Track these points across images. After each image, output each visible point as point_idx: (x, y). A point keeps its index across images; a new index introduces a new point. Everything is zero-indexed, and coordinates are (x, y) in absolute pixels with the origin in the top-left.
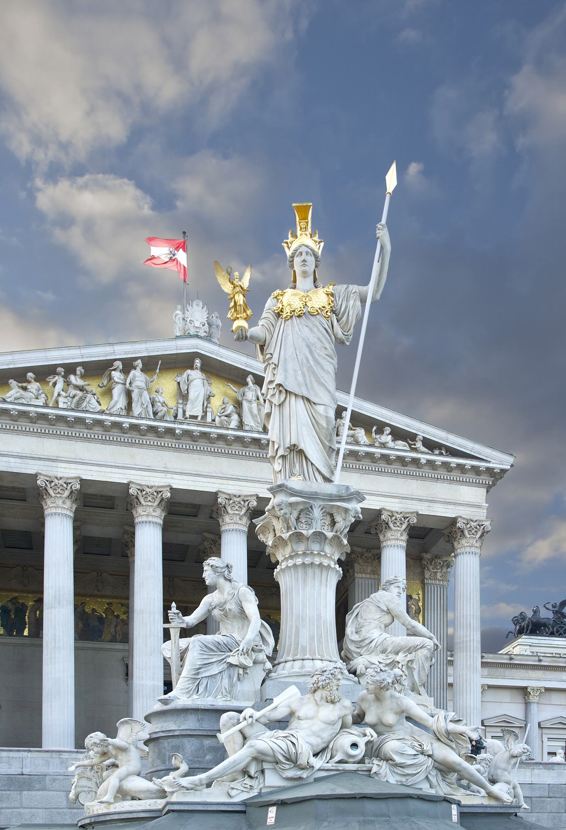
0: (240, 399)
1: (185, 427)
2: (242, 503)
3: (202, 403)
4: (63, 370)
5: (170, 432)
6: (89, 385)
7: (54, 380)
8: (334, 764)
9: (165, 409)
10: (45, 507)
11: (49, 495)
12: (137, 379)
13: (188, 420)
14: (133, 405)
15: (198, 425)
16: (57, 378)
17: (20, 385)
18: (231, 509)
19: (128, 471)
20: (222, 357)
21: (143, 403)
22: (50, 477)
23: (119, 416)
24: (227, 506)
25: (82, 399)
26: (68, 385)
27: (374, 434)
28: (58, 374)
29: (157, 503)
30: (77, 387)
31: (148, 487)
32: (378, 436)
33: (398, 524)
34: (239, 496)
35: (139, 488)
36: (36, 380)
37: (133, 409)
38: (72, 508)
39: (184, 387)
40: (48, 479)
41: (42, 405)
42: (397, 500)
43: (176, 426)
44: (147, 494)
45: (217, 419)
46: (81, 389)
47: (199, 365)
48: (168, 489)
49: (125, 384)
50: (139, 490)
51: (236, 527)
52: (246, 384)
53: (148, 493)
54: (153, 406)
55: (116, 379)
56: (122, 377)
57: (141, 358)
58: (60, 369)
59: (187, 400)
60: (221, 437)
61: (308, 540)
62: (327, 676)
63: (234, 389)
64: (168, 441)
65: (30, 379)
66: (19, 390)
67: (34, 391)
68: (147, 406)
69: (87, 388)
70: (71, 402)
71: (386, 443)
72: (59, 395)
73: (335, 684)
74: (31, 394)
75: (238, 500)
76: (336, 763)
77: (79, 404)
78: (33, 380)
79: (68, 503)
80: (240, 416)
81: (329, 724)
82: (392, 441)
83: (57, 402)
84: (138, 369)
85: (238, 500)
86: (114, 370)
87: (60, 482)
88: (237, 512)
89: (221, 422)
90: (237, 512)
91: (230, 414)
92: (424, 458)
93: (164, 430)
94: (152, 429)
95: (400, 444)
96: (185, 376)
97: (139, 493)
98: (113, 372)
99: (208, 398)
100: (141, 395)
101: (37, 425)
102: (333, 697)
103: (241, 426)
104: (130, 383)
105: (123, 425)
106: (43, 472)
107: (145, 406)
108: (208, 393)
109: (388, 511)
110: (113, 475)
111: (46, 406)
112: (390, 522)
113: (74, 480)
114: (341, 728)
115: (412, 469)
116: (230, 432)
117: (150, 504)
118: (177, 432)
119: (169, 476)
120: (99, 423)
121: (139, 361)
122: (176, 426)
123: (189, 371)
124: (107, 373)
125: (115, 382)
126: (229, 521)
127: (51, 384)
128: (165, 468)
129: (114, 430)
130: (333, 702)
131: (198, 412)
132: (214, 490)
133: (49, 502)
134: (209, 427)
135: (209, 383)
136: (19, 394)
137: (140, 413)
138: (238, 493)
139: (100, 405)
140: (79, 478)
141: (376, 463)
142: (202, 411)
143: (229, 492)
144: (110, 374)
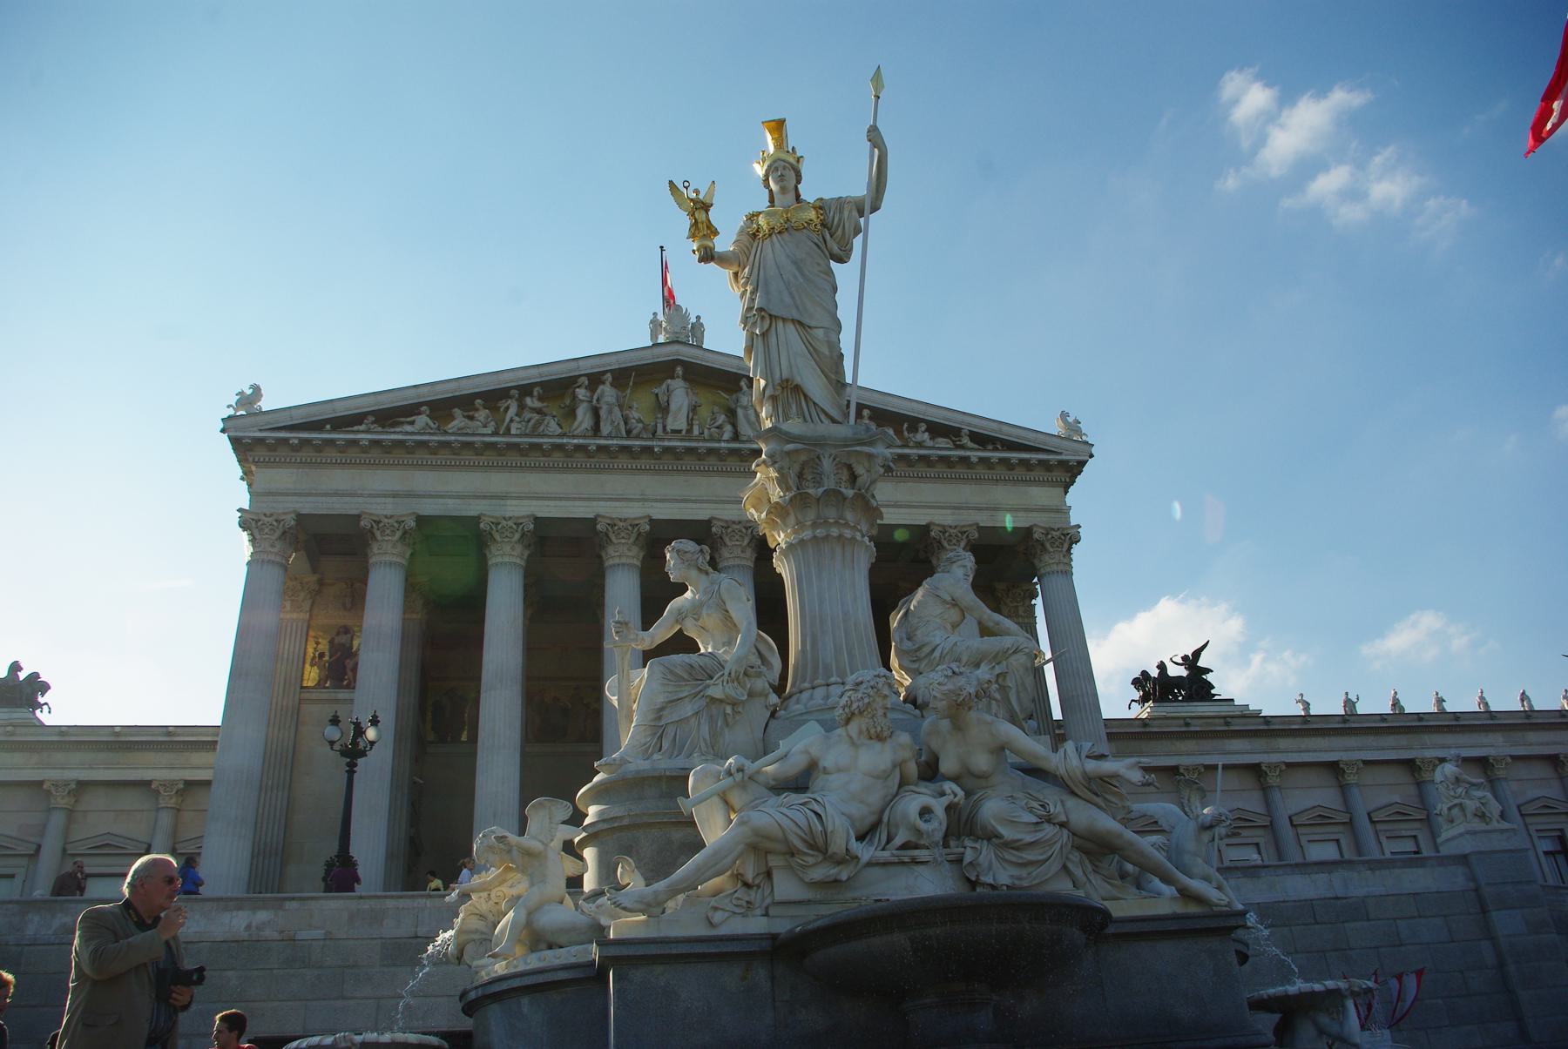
0: (734, 406)
1: (666, 443)
2: (744, 530)
3: (686, 415)
4: (516, 392)
5: (648, 450)
6: (547, 406)
7: (506, 405)
8: (895, 852)
9: (640, 425)
10: (489, 556)
11: (495, 540)
12: (606, 394)
14: (602, 424)
15: (681, 440)
16: (509, 401)
17: (466, 414)
18: (730, 540)
19: (595, 503)
20: (707, 362)
22: (496, 518)
23: (584, 437)
24: (724, 536)
25: (539, 423)
26: (523, 409)
27: (906, 433)
28: (511, 397)
29: (632, 540)
30: (534, 410)
31: (621, 520)
32: (911, 435)
33: (954, 541)
34: (740, 522)
35: (609, 522)
36: (485, 408)
38: (523, 555)
39: (662, 399)
40: (493, 520)
41: (490, 432)
42: (949, 511)
43: (655, 443)
45: (706, 431)
46: (539, 411)
47: (680, 373)
48: (647, 520)
49: (591, 402)
50: (609, 525)
51: (738, 562)
52: (741, 389)
54: (626, 423)
55: (580, 397)
56: (588, 394)
57: (610, 371)
58: (513, 392)
59: (668, 413)
60: (711, 451)
61: (818, 504)
62: (865, 691)
63: (725, 396)
64: (644, 462)
65: (478, 406)
66: (464, 419)
67: (482, 420)
68: (618, 424)
69: (544, 410)
70: (526, 427)
71: (924, 441)
72: (512, 420)
73: (880, 705)
74: (478, 423)
75: (738, 527)
76: (897, 849)
77: (535, 427)
78: (481, 408)
79: (519, 548)
80: (734, 426)
81: (878, 777)
82: (931, 439)
83: (508, 429)
84: (608, 383)
85: (738, 527)
86: (579, 387)
87: (509, 522)
88: (737, 543)
89: (711, 435)
90: (737, 543)
91: (721, 425)
92: (975, 455)
94: (625, 449)
95: (942, 442)
96: (664, 386)
97: (610, 529)
98: (577, 390)
99: (694, 409)
100: (610, 412)
101: (483, 457)
102: (879, 729)
103: (736, 437)
104: (598, 400)
105: (590, 448)
106: (488, 513)
107: (616, 423)
108: (694, 403)
109: (938, 525)
111: (495, 434)
112: (943, 540)
113: (527, 519)
114: (900, 786)
115: (960, 470)
116: (723, 445)
117: (623, 541)
118: (656, 450)
120: (559, 447)
121: (609, 375)
122: (655, 443)
123: (669, 381)
124: (571, 390)
126: (728, 555)
127: (502, 409)
129: (577, 455)
130: (880, 738)
131: (681, 424)
132: (706, 517)
133: (493, 548)
134: (698, 441)
135: (694, 393)
136: (463, 424)
137: (611, 432)
138: (735, 518)
139: (561, 428)
140: (533, 515)
141: (913, 466)
142: (686, 423)
143: (726, 518)
144: (574, 391)
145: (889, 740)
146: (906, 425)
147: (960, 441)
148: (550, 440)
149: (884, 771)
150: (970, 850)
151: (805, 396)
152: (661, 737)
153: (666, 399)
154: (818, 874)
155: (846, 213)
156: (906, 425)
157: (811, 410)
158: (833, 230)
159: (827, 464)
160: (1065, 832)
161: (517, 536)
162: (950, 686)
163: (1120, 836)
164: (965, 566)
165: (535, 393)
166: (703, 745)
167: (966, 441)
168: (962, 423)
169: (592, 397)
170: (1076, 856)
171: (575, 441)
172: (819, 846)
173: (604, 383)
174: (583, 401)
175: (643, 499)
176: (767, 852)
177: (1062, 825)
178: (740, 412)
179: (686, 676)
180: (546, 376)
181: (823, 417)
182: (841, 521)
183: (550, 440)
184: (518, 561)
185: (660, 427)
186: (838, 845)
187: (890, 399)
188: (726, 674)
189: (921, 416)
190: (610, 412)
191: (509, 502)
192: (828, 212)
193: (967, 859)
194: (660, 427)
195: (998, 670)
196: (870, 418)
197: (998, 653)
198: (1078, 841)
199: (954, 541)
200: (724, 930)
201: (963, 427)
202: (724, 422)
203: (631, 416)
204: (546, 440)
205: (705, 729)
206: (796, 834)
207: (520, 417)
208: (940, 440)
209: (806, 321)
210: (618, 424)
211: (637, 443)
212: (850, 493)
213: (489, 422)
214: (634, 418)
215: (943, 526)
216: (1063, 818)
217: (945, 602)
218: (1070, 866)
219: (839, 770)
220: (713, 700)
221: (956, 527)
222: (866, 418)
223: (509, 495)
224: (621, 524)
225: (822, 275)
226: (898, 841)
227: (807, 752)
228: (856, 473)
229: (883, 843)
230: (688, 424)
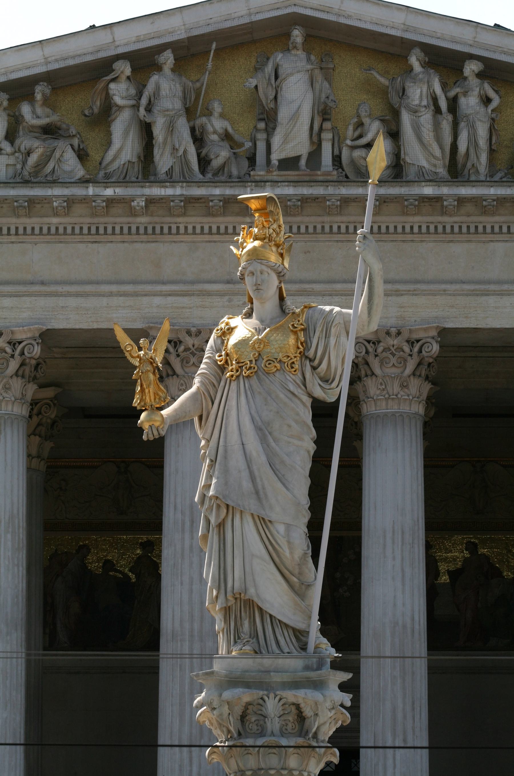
13: (275, 173)
14: (156, 151)
15: (296, 183)
21: (177, 146)
44: (187, 349)
49: (136, 107)
53: (191, 346)
55: (118, 100)
68: (185, 152)
86: (114, 80)
98: (112, 86)
100: (171, 128)
107: (181, 152)
124: (101, 85)
153: (272, 97)
155: (332, 341)
157: (265, 624)
158: (316, 362)
161: (13, 365)
165: (39, 96)
169: (140, 95)
171: (109, 192)
173: (159, 68)
178: (406, 118)
180: (57, 60)
183: (66, 192)
185: (261, 146)
190: (171, 128)
192: (312, 335)
194: (261, 146)
203: (210, 129)
204: (57, 191)
207: (12, 143)
210: (185, 152)
211: (217, 191)
214: (215, 132)
228: (304, 715)
230: (312, 142)
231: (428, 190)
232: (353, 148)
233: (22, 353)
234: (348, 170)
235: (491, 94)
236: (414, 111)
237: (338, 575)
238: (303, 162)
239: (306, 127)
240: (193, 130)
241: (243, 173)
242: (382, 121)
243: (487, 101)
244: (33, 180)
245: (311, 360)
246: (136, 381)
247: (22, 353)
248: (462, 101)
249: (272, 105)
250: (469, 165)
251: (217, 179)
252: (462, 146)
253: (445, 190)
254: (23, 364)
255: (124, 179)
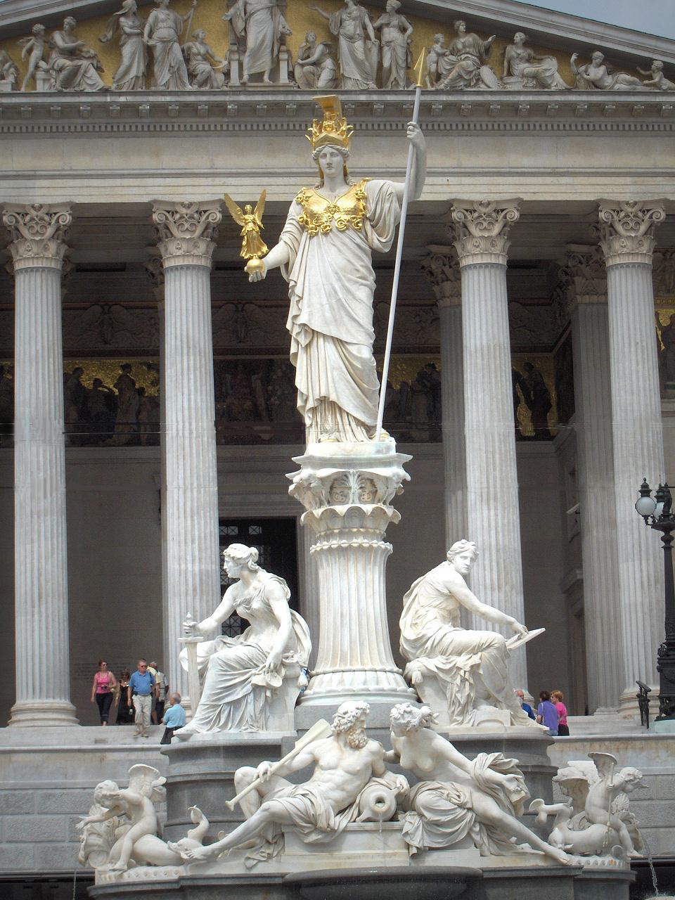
1: (243, 98)
12: (161, 25)
14: (156, 69)
37: (156, 76)
49: (141, 34)
50: (168, 212)
55: (127, 30)
56: (137, 23)
68: (178, 69)
93: (207, 107)
98: (122, 19)
100: (167, 51)
104: (150, 36)
107: (176, 69)
110: (126, 191)
118: (229, 107)
119: (218, 181)
125: (125, 33)
128: (211, 168)
145: (364, 749)
146: (574, 57)
147: (650, 77)
148: (90, 99)
149: (359, 771)
150: (409, 822)
151: (340, 409)
152: (219, 714)
154: (314, 837)
156: (574, 57)
159: (353, 483)
160: (470, 815)
161: (50, 231)
162: (402, 721)
163: (500, 820)
164: (465, 558)
166: (249, 719)
167: (657, 77)
168: (654, 51)
170: (477, 829)
171: (122, 99)
172: (312, 821)
174: (129, 35)
175: (214, 174)
176: (280, 824)
177: (470, 809)
178: (343, 43)
179: (238, 667)
181: (353, 424)
182: (362, 530)
183: (90, 99)
184: (53, 265)
186: (322, 823)
187: (555, 19)
188: (267, 666)
189: (597, 42)
191: (39, 183)
192: (371, 201)
193: (404, 831)
195: (471, 662)
196: (526, 44)
197: (474, 647)
198: (479, 819)
199: (632, 224)
200: (255, 871)
201: (655, 57)
202: (323, 55)
203: (194, 50)
205: (250, 707)
206: (297, 815)
208: (624, 76)
209: (345, 338)
210: (178, 69)
212: (368, 508)
213: (7, 70)
214: (199, 54)
215: (619, 203)
216: (469, 805)
217: (442, 594)
218: (473, 835)
219: (330, 768)
220: (256, 688)
221: (635, 203)
222: (520, 45)
223: (38, 173)
224: (184, 211)
225: (360, 280)
226: (364, 816)
227: (311, 753)
229: (355, 817)
230: (273, 62)
231: (363, 98)
232: (302, 66)
233: (57, 221)
234: (300, 82)
235: (407, 24)
236: (351, 38)
237: (270, 388)
238: (266, 77)
239: (269, 50)
240: (183, 51)
241: (221, 84)
242: (326, 45)
243: (403, 30)
244: (65, 90)
245: (370, 221)
246: (243, 237)
247: (57, 221)
248: (386, 30)
249: (243, 34)
250: (392, 79)
251: (203, 89)
252: (386, 64)
253: (375, 98)
254: (58, 230)
255: (133, 89)
